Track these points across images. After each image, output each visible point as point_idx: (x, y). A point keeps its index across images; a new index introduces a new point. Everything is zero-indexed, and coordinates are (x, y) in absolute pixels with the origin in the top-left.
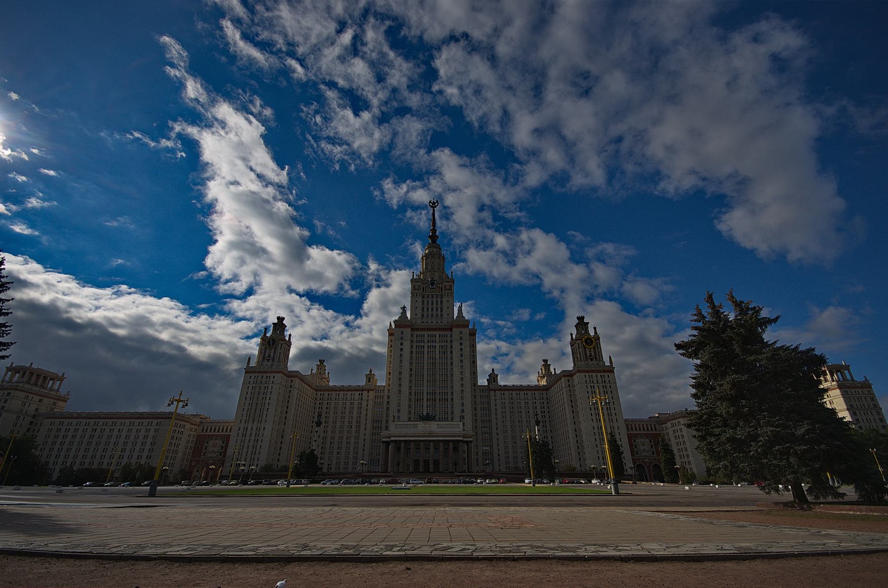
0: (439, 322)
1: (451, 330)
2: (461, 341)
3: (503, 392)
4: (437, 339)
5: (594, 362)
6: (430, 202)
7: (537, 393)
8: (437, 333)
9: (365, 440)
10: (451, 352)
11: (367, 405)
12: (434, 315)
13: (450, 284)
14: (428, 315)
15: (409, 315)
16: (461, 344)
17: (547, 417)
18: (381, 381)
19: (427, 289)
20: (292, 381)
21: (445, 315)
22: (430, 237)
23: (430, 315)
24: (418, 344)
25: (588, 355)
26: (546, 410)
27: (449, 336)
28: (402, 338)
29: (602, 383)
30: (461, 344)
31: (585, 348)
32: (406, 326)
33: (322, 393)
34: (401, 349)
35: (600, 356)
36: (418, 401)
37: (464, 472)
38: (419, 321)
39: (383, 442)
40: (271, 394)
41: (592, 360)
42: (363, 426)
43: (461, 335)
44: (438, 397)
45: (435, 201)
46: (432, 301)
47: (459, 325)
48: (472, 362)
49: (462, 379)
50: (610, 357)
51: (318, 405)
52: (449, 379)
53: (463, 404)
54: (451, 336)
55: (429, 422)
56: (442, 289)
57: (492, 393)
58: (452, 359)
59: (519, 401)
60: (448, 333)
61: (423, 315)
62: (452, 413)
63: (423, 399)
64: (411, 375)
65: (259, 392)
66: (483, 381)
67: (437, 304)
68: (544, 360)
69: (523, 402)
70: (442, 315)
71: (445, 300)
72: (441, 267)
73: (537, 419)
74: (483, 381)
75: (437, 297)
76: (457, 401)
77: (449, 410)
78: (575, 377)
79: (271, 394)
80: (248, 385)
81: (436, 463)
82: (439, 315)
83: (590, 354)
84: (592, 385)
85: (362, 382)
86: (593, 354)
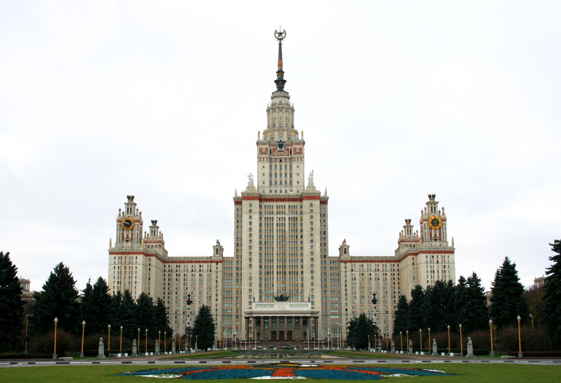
0: (288, 191)
2: (311, 214)
3: (353, 264)
4: (287, 209)
5: (438, 243)
6: (276, 31)
7: (388, 264)
8: (287, 204)
9: (217, 310)
10: (302, 224)
11: (217, 276)
12: (283, 183)
13: (301, 146)
14: (276, 182)
15: (256, 185)
16: (312, 217)
17: (397, 288)
18: (229, 252)
19: (275, 153)
20: (150, 259)
21: (294, 183)
22: (276, 82)
23: (278, 183)
24: (267, 216)
25: (433, 235)
26: (396, 281)
28: (250, 211)
29: (442, 263)
30: (312, 217)
31: (431, 228)
32: (253, 198)
33: (170, 264)
34: (250, 223)
35: (445, 237)
36: (268, 274)
37: (313, 338)
38: (267, 192)
39: (245, 318)
40: (136, 274)
41: (436, 240)
42: (214, 297)
43: (311, 208)
44: (287, 271)
45: (282, 32)
46: (281, 166)
47: (310, 196)
48: (322, 233)
49: (312, 253)
50: (453, 238)
51: (167, 277)
52: (299, 252)
53: (312, 277)
54: (301, 207)
55: (284, 303)
56: (291, 151)
57: (343, 265)
58: (302, 231)
59: (370, 272)
60: (298, 204)
61: (271, 182)
62: (302, 286)
63: (273, 272)
64: (260, 248)
65: (125, 272)
66: (333, 251)
68: (406, 221)
70: (291, 182)
71: (294, 165)
72: (290, 123)
73: (374, 298)
74: (333, 251)
75: (286, 161)
76: (307, 275)
77: (299, 282)
78: (418, 256)
79: (136, 274)
80: (114, 265)
81: (290, 333)
82: (288, 183)
83: (435, 235)
84: (432, 265)
85: (209, 253)
86: (438, 235)
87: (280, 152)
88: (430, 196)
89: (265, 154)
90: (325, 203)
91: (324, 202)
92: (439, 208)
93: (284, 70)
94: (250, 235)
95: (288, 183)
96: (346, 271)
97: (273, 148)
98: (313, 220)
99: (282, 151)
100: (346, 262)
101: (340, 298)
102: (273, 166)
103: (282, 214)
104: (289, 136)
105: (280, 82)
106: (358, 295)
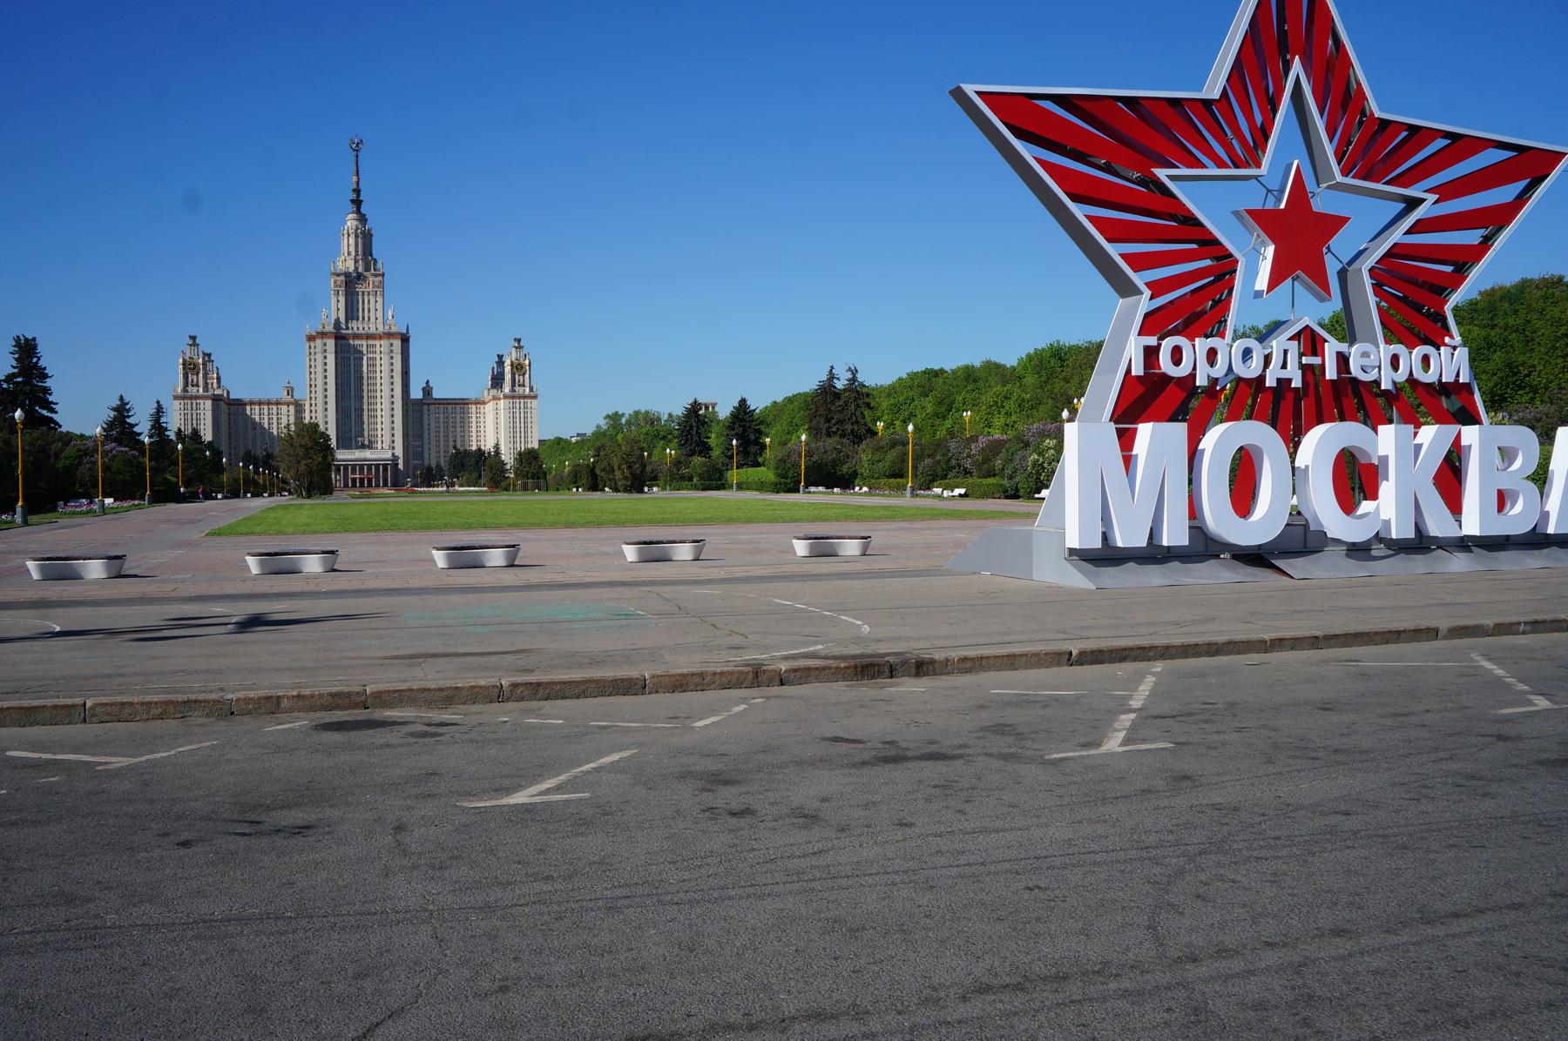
1: (381, 338)
8: (364, 342)
13: (380, 278)
16: (392, 358)
27: (378, 346)
28: (325, 351)
34: (325, 364)
41: (519, 386)
57: (426, 407)
60: (377, 343)
66: (416, 393)
68: (498, 356)
69: (458, 416)
74: (416, 393)
78: (502, 401)
82: (366, 318)
86: (522, 380)
88: (515, 339)
91: (405, 340)
92: (525, 351)
93: (361, 187)
94: (326, 377)
95: (366, 318)
96: (429, 415)
98: (393, 361)
100: (429, 404)
101: (422, 442)
105: (357, 203)
106: (442, 439)
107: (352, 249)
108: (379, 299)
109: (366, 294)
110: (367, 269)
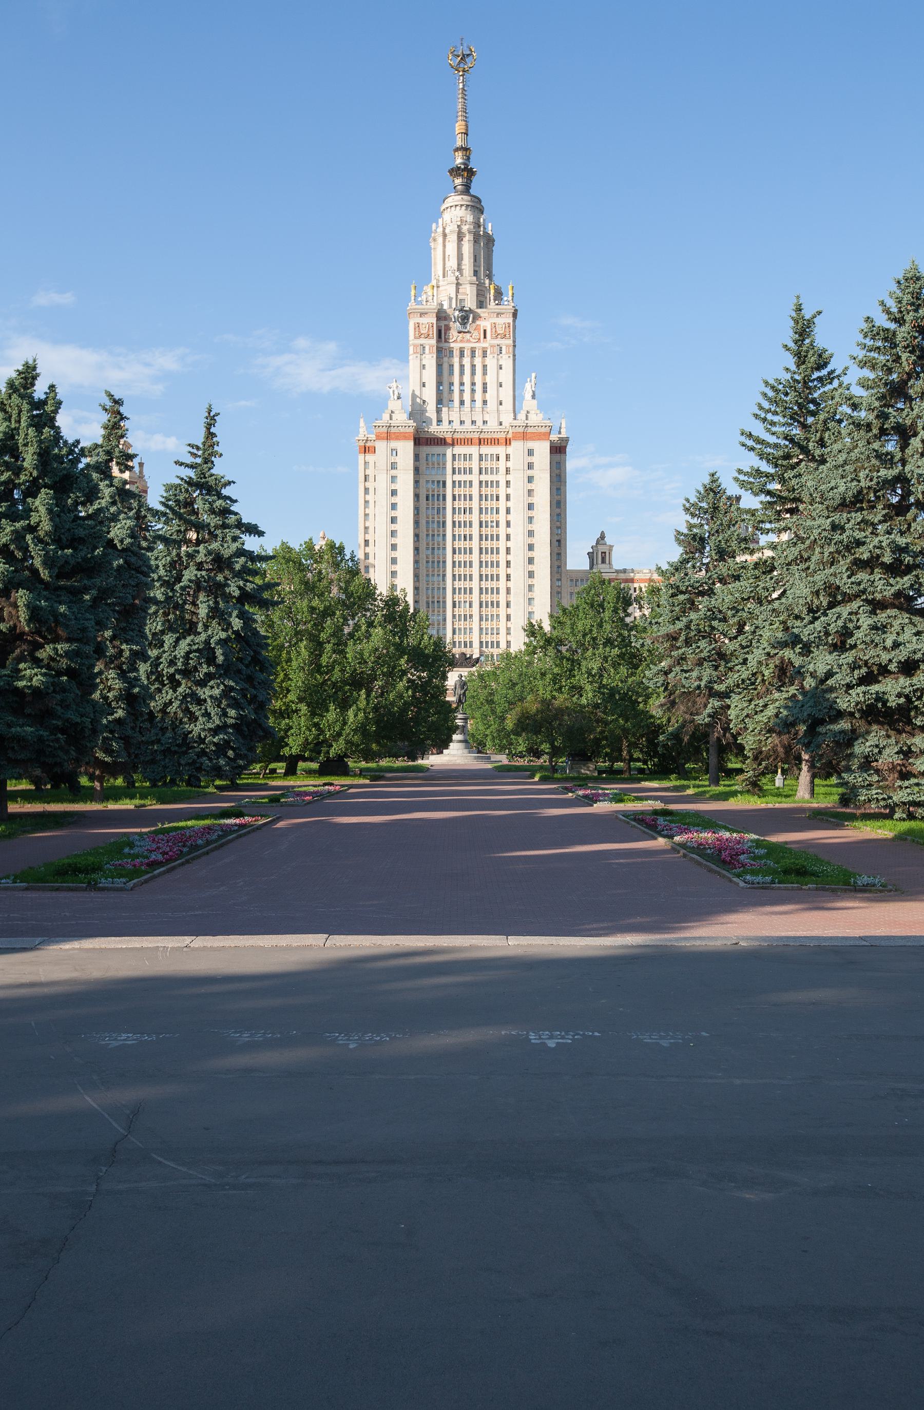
0: (479, 423)
1: (507, 442)
2: (530, 473)
28: (394, 466)
54: (508, 457)
56: (485, 331)
60: (500, 450)
61: (439, 401)
67: (473, 373)
82: (479, 403)
87: (461, 335)
89: (427, 336)
90: (560, 452)
95: (479, 403)
97: (445, 325)
99: (464, 332)
102: (446, 367)
103: (465, 473)
104: (482, 299)
107: (452, 263)
108: (507, 363)
109: (478, 353)
110: (481, 304)
